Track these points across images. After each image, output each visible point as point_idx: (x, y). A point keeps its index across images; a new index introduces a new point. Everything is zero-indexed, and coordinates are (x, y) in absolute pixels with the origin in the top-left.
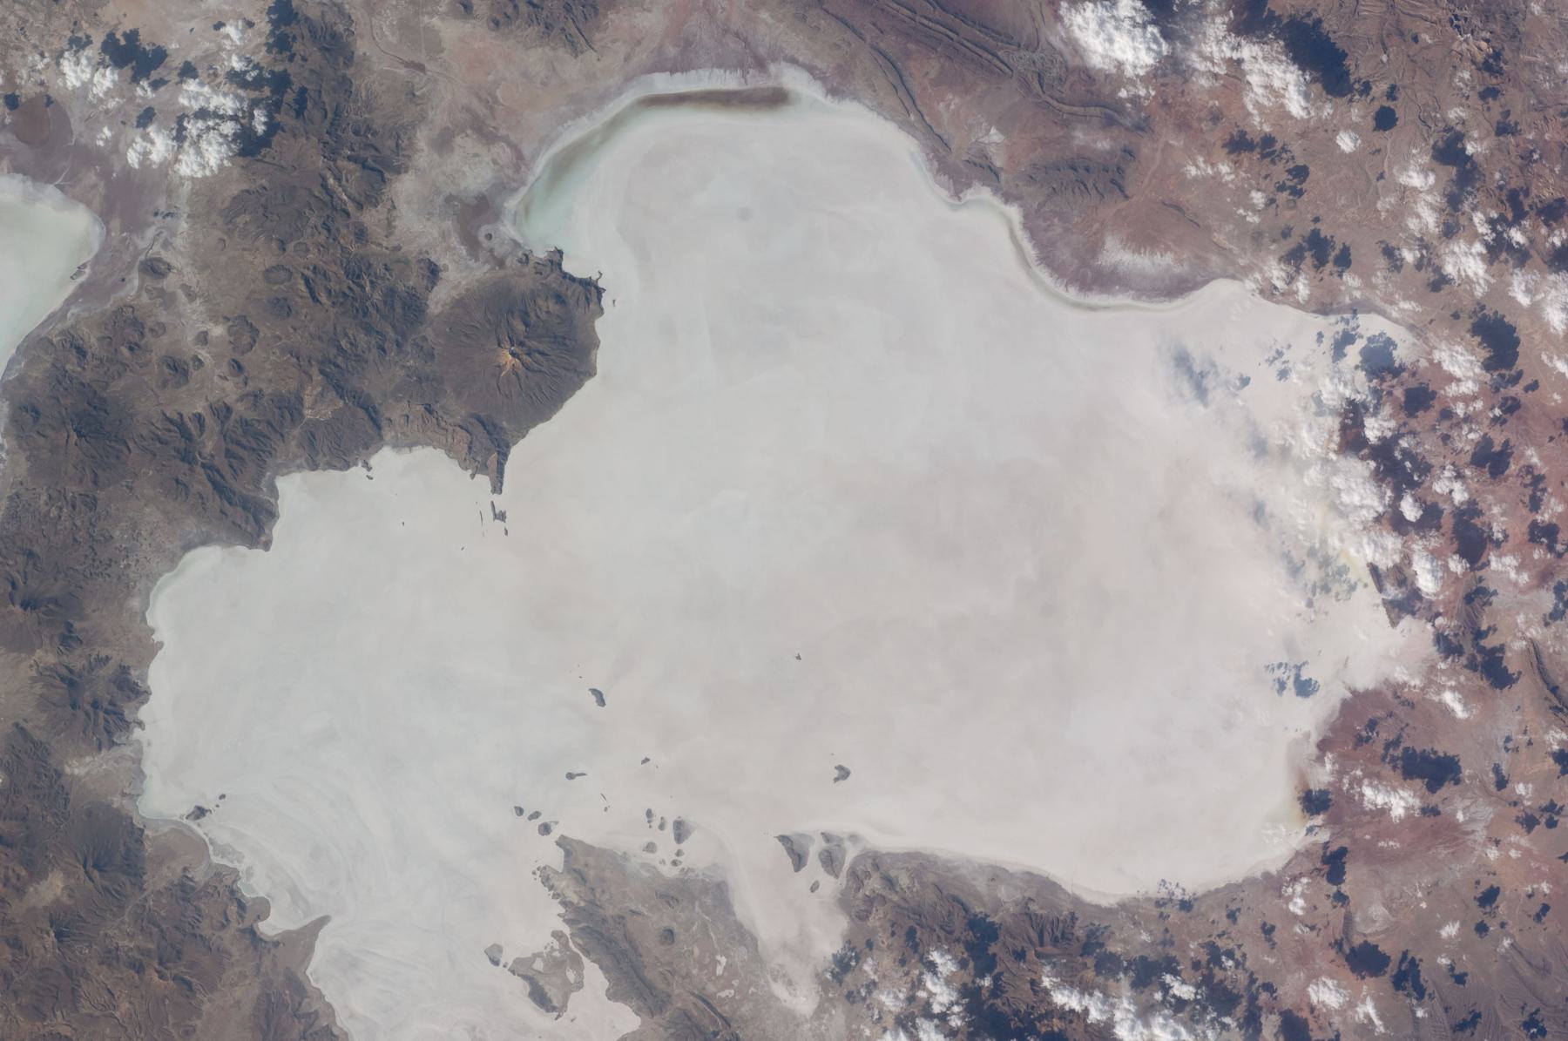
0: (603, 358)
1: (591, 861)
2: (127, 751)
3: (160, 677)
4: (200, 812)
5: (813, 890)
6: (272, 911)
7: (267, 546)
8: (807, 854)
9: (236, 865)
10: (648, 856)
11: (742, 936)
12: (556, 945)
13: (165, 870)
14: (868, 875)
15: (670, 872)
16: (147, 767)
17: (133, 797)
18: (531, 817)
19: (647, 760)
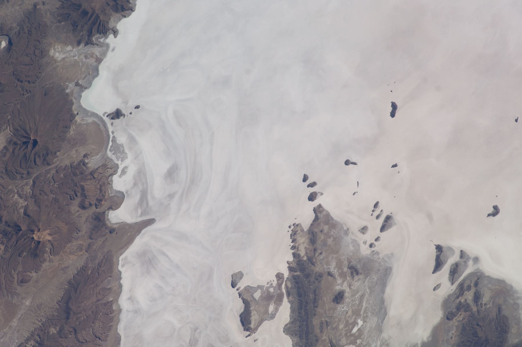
1: (326, 228)
2: (97, 51)
4: (117, 114)
5: (435, 289)
6: (123, 206)
8: (446, 262)
9: (119, 163)
10: (360, 235)
11: (381, 310)
12: (275, 283)
13: (73, 153)
14: (469, 288)
15: (365, 251)
16: (101, 67)
17: (83, 88)
18: (309, 186)
19: (395, 166)
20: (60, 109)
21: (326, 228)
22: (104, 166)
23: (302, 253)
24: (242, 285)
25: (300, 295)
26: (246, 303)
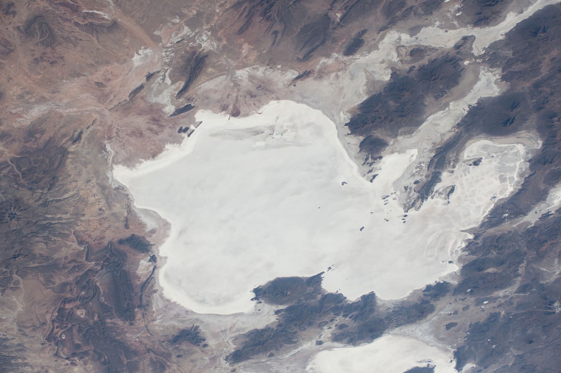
0: (272, 279)
1: (407, 205)
3: (422, 286)
4: (450, 262)
7: (373, 292)
20: (466, 269)
21: (407, 205)
22: (464, 251)
23: (420, 201)
24: (447, 201)
25: (429, 189)
26: (448, 195)
